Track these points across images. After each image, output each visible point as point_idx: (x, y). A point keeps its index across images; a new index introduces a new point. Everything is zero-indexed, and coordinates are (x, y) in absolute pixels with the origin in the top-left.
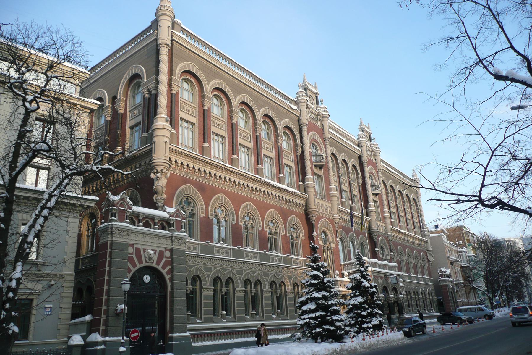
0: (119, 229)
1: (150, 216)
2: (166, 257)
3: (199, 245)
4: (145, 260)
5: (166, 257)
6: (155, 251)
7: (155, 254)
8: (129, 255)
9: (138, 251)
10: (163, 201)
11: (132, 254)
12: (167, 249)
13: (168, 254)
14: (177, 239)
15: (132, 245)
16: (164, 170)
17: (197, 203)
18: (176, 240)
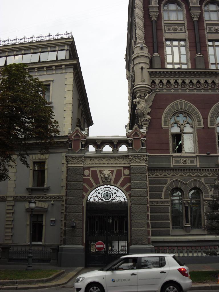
0: (73, 157)
1: (108, 141)
2: (125, 175)
3: (198, 158)
4: (102, 180)
5: (125, 175)
6: (112, 171)
7: (112, 173)
8: (84, 177)
9: (94, 173)
10: (147, 123)
11: (89, 176)
12: (125, 168)
13: (127, 172)
14: (134, 157)
15: (88, 168)
16: (143, 94)
17: (192, 115)
18: (134, 158)
